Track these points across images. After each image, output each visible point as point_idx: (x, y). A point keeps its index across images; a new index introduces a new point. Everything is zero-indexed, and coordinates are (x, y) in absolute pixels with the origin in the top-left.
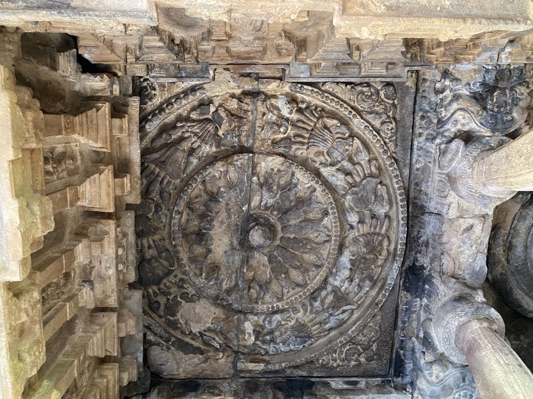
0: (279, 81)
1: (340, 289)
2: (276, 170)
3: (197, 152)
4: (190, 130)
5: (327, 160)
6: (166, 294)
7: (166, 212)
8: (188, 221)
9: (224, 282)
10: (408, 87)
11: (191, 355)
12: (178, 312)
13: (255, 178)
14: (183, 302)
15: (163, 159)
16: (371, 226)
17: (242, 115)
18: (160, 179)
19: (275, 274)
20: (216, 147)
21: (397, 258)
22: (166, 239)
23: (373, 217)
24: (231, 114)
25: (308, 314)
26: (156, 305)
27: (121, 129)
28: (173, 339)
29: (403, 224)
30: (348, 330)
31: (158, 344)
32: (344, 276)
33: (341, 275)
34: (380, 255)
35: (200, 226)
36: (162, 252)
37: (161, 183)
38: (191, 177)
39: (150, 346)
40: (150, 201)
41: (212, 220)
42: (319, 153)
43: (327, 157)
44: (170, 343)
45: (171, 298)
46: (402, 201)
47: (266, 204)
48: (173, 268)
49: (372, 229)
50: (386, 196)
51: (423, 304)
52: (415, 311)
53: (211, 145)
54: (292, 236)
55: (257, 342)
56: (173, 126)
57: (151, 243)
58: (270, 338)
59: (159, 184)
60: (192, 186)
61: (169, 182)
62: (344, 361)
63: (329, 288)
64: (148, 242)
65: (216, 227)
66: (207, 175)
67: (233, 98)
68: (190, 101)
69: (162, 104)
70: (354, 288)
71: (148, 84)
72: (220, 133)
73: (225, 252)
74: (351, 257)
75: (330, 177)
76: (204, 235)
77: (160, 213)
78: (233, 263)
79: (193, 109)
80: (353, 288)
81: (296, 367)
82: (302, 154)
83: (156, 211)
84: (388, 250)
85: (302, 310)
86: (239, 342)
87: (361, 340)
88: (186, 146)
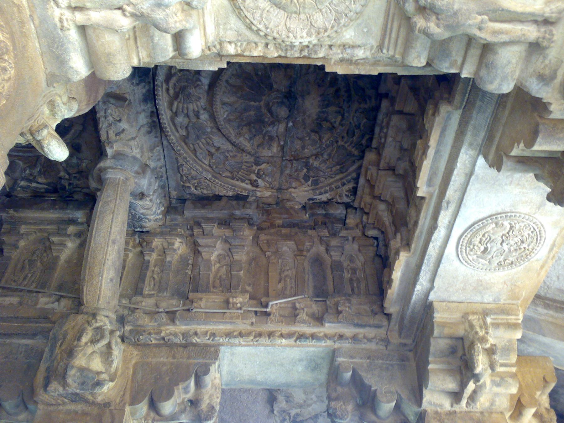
10: (175, 191)
13: (282, 143)
18: (353, 145)
20: (309, 162)
23: (187, 116)
24: (297, 179)
41: (317, 119)
42: (235, 156)
43: (228, 155)
46: (166, 128)
47: (273, 127)
49: (185, 106)
50: (179, 129)
54: (252, 103)
61: (346, 143)
72: (305, 170)
75: (224, 142)
82: (247, 156)
83: (360, 124)
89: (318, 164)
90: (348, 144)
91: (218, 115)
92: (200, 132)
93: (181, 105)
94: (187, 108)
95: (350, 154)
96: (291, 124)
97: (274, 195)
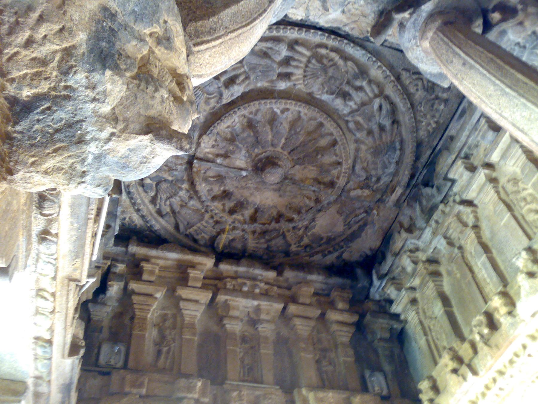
2: (214, 143)
11: (363, 234)
41: (247, 201)
53: (181, 189)
54: (283, 141)
61: (207, 222)
62: (433, 116)
80: (358, 97)
92: (260, 74)
94: (297, 67)
96: (244, 173)
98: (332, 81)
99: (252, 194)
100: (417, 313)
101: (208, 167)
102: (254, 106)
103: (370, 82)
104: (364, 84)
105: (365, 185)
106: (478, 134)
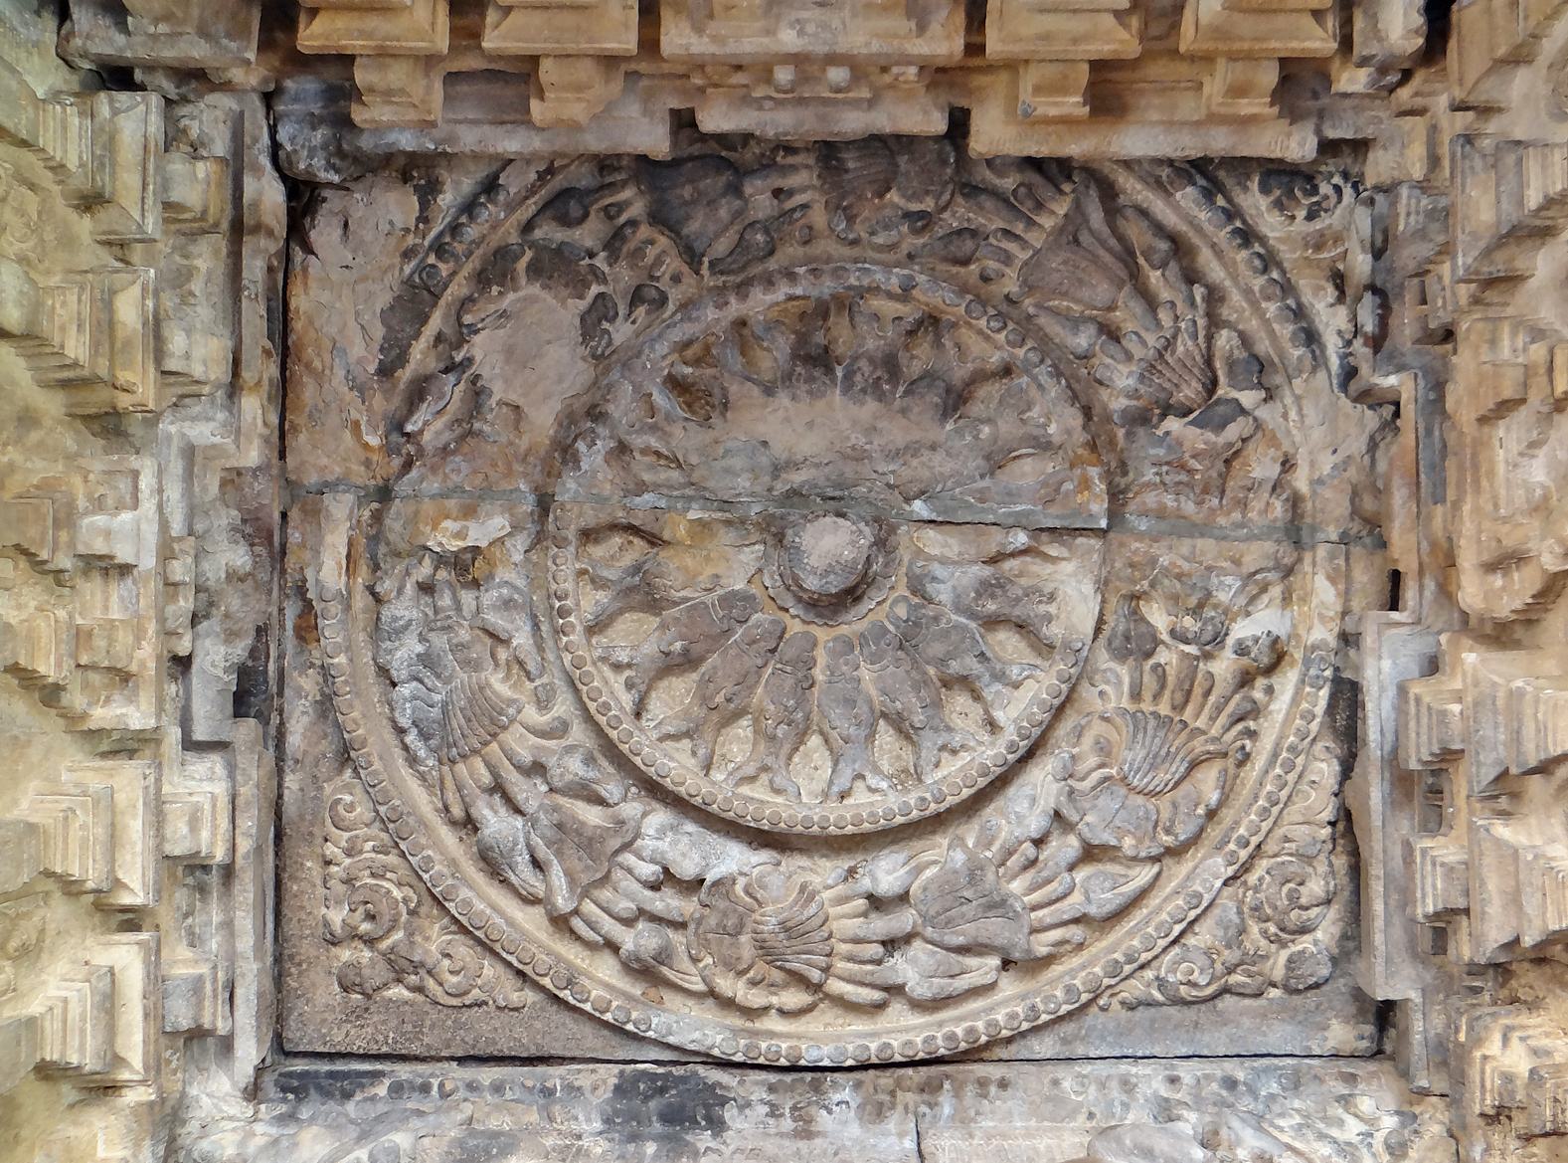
0: (1339, 609)
1: (626, 847)
2: (1052, 609)
3: (1112, 348)
4: (1183, 325)
5: (1083, 779)
6: (614, 243)
7: (905, 248)
8: (876, 317)
9: (660, 438)
12: (544, 287)
14: (583, 305)
15: (1085, 238)
16: (857, 941)
17: (1229, 493)
18: (1019, 228)
19: (684, 619)
21: (743, 1042)
22: (807, 248)
25: (533, 740)
26: (575, 210)
27: (1238, 91)
28: (444, 269)
29: (867, 1048)
30: (471, 887)
31: (424, 218)
32: (679, 859)
33: (681, 846)
34: (754, 983)
35: (855, 358)
36: (767, 232)
37: (1007, 233)
38: (1026, 330)
39: (417, 188)
40: (946, 197)
41: (881, 397)
44: (432, 259)
45: (600, 261)
47: (934, 579)
48: (705, 270)
51: (585, 1143)
52: (551, 1119)
54: (819, 674)
55: (427, 561)
56: (1191, 277)
57: (799, 199)
58: (443, 609)
59: (1002, 225)
60: (999, 331)
61: (1007, 259)
63: (631, 809)
64: (803, 189)
65: (854, 409)
66: (1035, 379)
67: (1283, 464)
68: (1276, 326)
69: (1263, 240)
70: (629, 896)
71: (1326, 197)
73: (765, 443)
74: (741, 882)
76: (829, 371)
77: (905, 229)
78: (728, 471)
79: (1245, 340)
80: (628, 893)
81: (326, 706)
83: (908, 215)
84: (766, 1009)
85: (547, 718)
86: (432, 497)
87: (427, 939)
88: (1128, 315)
89: (1124, 369)
90: (1012, 247)
91: (872, 814)
93: (840, 966)
95: (1070, 234)
97: (1332, 557)
98: (730, 923)
99: (872, 430)
100: (58, 169)
101: (1053, 510)
102: (949, 777)
103: (612, 947)
104: (628, 939)
105: (466, 567)
106: (215, 980)
